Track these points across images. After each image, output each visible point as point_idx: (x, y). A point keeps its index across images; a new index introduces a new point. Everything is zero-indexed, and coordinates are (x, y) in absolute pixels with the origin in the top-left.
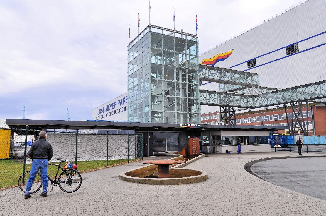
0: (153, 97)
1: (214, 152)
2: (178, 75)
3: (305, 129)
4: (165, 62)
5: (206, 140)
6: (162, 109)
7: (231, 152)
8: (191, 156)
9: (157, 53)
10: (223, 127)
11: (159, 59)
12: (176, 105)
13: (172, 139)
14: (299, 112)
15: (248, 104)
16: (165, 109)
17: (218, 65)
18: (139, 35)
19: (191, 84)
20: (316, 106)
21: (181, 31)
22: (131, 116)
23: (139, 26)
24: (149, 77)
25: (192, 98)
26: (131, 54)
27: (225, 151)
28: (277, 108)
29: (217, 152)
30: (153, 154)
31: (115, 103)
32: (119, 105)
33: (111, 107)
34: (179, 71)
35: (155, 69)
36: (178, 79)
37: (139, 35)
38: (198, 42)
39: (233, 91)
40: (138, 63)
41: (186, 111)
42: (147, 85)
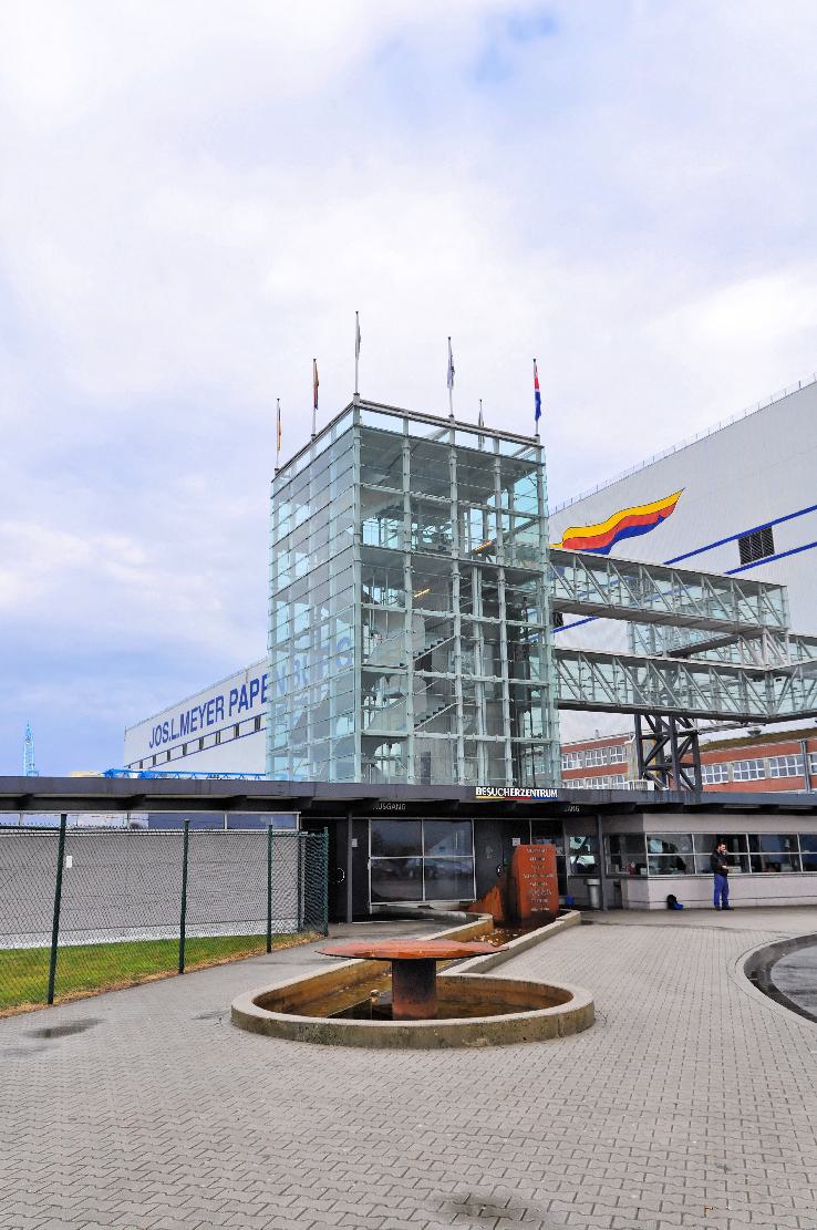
0: (369, 680)
1: (617, 905)
2: (466, 590)
4: (414, 541)
5: (577, 853)
6: (405, 726)
7: (686, 905)
8: (526, 919)
10: (651, 800)
11: (393, 531)
12: (460, 712)
13: (450, 850)
15: (747, 707)
16: (415, 726)
17: (623, 550)
18: (316, 438)
19: (518, 628)
21: (476, 424)
22: (285, 755)
23: (316, 406)
24: (355, 597)
25: (527, 682)
26: (285, 510)
27: (663, 897)
29: (632, 905)
30: (371, 909)
31: (220, 702)
33: (202, 715)
34: (470, 576)
35: (378, 568)
36: (468, 609)
37: (316, 438)
38: (543, 465)
39: (685, 653)
40: (311, 544)
41: (502, 734)
42: (344, 630)
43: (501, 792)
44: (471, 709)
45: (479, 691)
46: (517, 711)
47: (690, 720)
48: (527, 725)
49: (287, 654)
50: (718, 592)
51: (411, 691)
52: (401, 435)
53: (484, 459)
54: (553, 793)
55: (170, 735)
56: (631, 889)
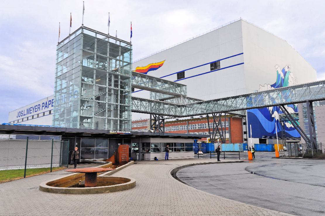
0: (83, 102)
1: (143, 159)
2: (110, 80)
3: (223, 137)
4: (97, 66)
5: (135, 147)
6: (92, 114)
7: (159, 159)
9: (89, 56)
10: (152, 134)
11: (91, 63)
12: (107, 111)
13: (103, 146)
14: (219, 123)
16: (95, 114)
17: (150, 74)
18: (70, 35)
19: (123, 91)
20: (233, 117)
21: (115, 37)
22: (58, 121)
23: (71, 26)
24: (79, 80)
26: (61, 54)
28: (201, 118)
29: (146, 159)
30: (80, 162)
32: (44, 108)
33: (33, 109)
34: (111, 76)
35: (87, 72)
36: (110, 85)
37: (70, 35)
38: (132, 50)
39: (163, 100)
41: (117, 117)
42: (77, 89)
43: (116, 132)
44: (109, 111)
45: (112, 106)
46: (121, 112)
47: (163, 116)
48: (124, 115)
49: (60, 94)
50: (172, 86)
51: (94, 105)
52: (94, 37)
53: (118, 47)
54: (129, 132)
55: (23, 114)
56: (146, 155)
